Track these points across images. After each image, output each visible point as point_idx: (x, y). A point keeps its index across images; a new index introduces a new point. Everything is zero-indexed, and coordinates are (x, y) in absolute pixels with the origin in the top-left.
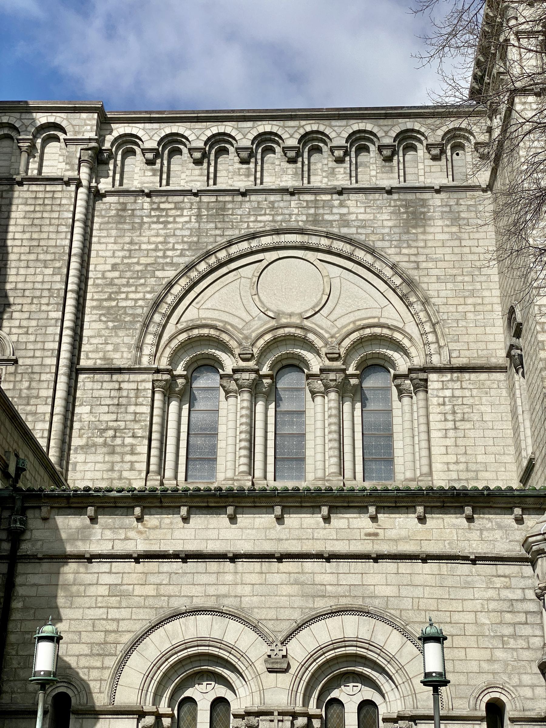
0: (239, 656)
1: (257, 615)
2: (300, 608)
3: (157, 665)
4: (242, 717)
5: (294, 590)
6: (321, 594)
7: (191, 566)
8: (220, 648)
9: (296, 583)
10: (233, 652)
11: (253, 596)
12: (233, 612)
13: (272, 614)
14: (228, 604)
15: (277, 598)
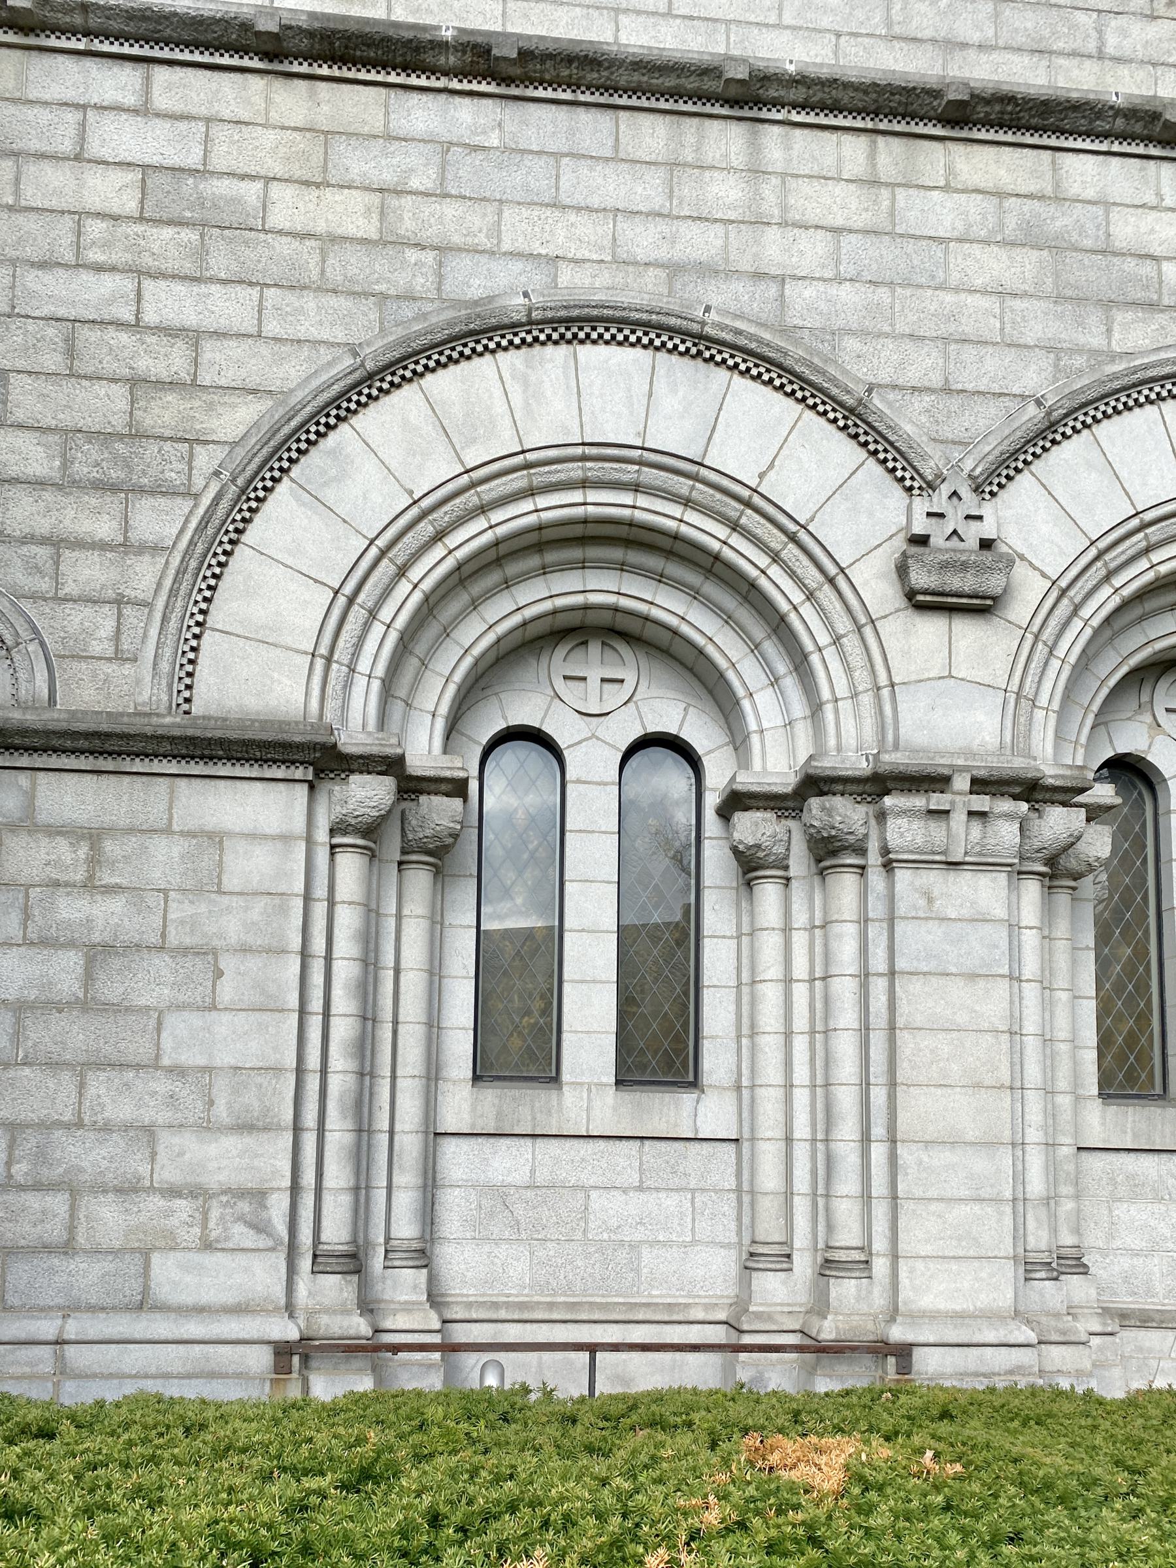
0: (776, 539)
1: (858, 366)
2: (1050, 349)
3: (390, 553)
4: (785, 804)
5: (1022, 268)
6: (1140, 295)
7: (543, 124)
8: (687, 502)
9: (1029, 239)
10: (749, 519)
11: (839, 280)
12: (751, 337)
13: (923, 365)
14: (723, 304)
15: (949, 298)
